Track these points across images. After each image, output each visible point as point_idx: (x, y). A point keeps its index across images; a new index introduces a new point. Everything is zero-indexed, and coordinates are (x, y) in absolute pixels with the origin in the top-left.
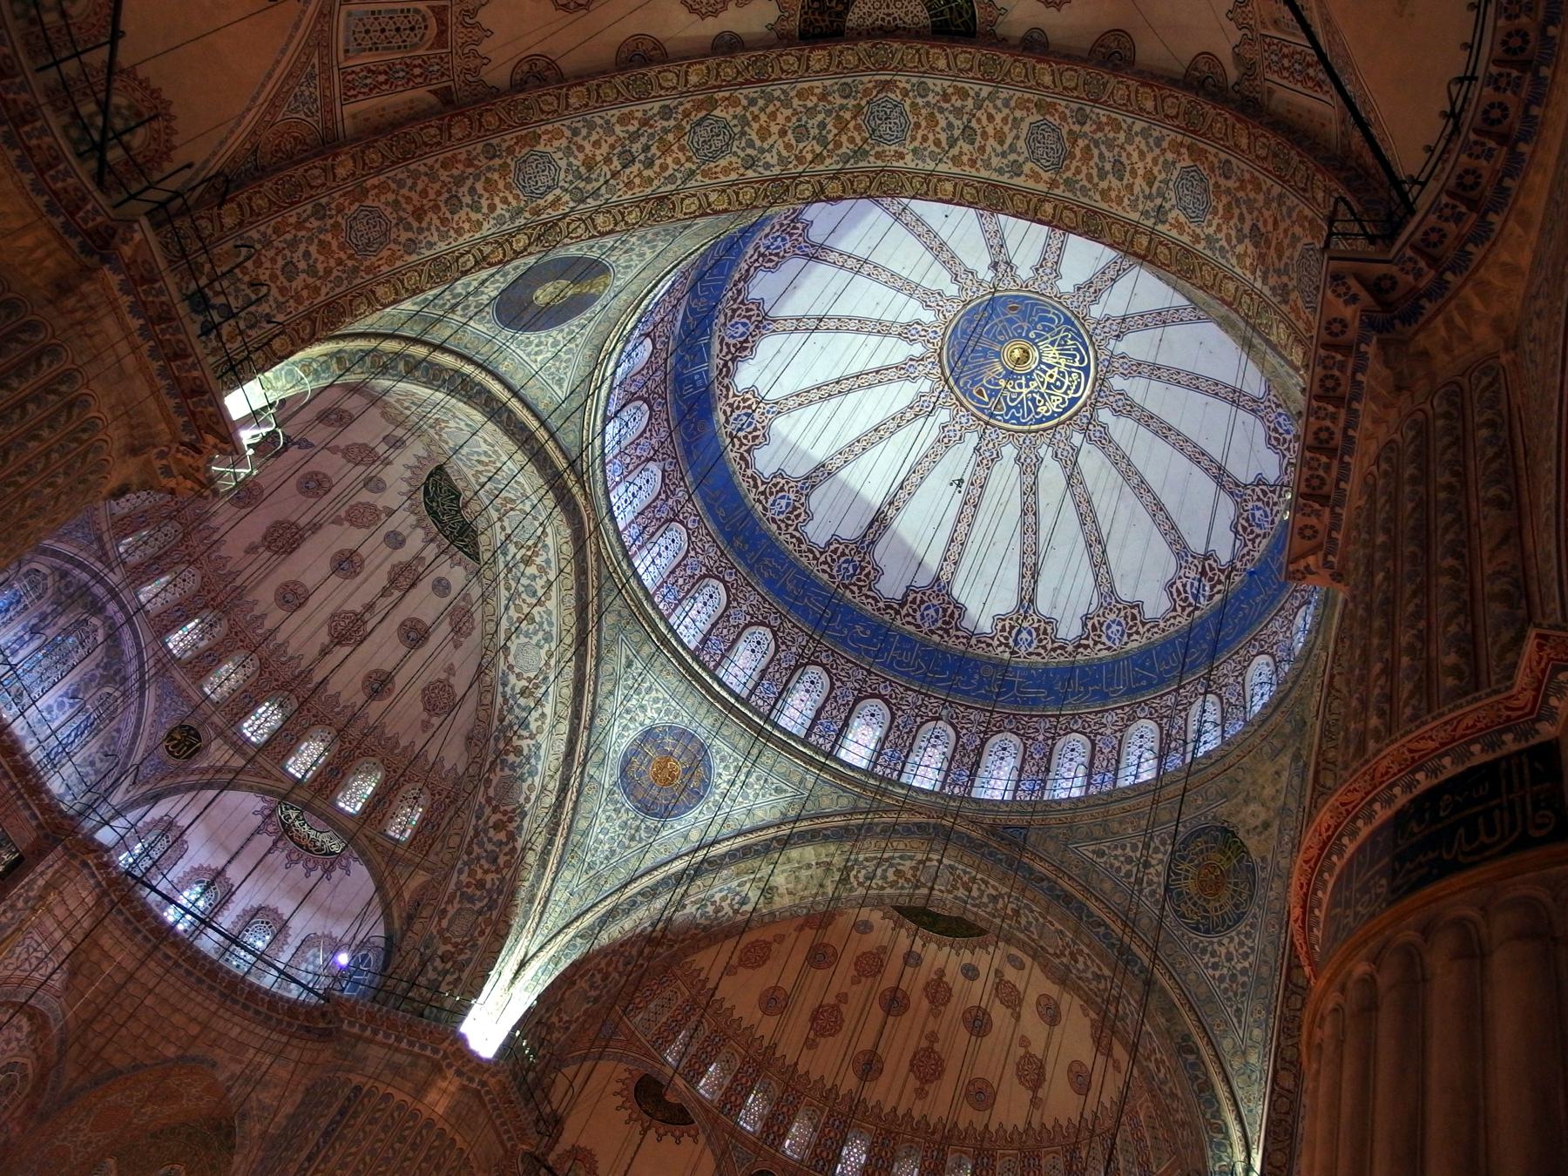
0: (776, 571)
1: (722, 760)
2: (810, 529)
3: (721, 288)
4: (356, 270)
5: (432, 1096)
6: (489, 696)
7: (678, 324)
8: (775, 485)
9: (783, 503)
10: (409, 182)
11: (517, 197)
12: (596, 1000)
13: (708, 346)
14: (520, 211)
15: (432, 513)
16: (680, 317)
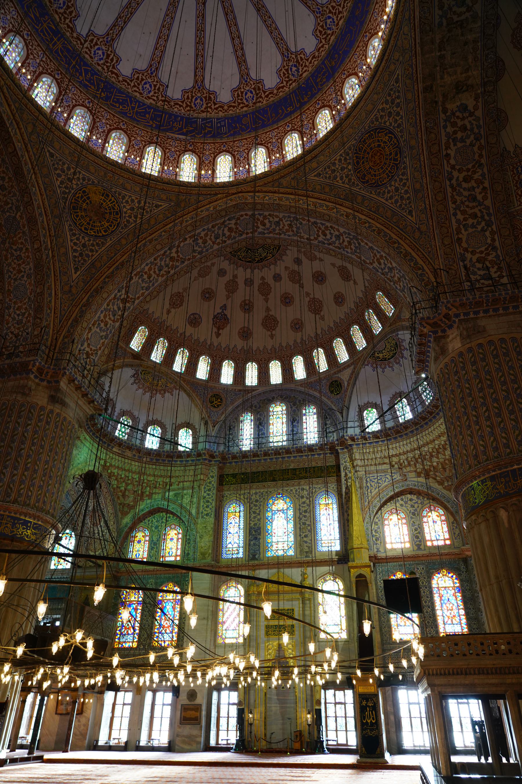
0: (323, 75)
1: (377, 121)
2: (308, 51)
3: (171, 115)
4: (29, 298)
5: (450, 347)
6: (331, 251)
7: (184, 137)
8: (284, 74)
9: (294, 69)
10: (10, 273)
11: (19, 233)
12: (489, 224)
13: (203, 119)
14: (24, 233)
15: (261, 260)
16: (181, 137)
